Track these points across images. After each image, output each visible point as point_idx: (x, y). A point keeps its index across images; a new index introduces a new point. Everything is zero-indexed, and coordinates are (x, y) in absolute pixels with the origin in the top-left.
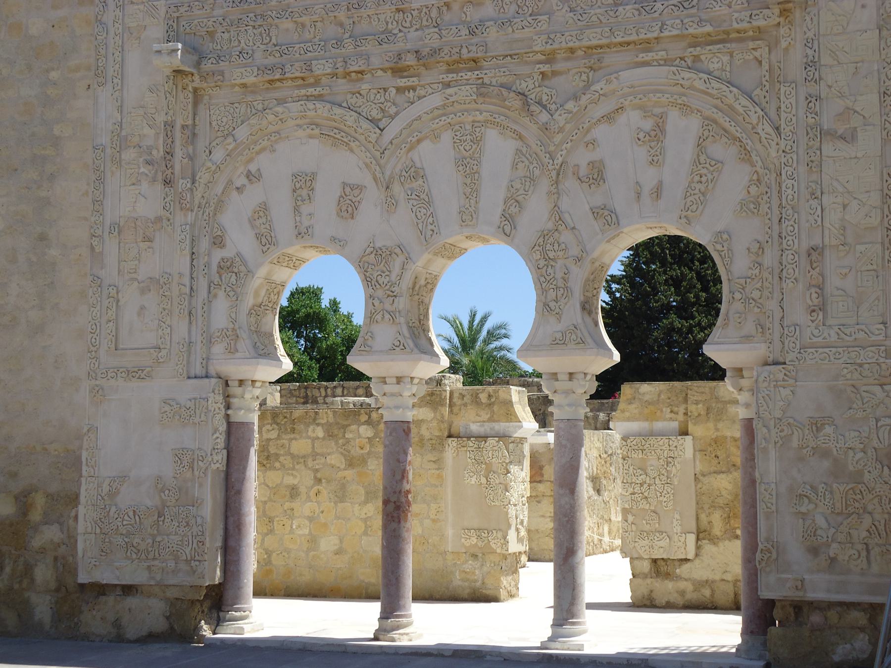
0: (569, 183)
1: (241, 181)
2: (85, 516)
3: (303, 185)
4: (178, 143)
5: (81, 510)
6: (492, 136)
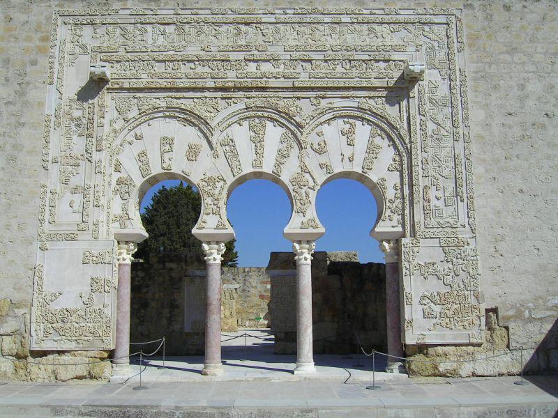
1: (130, 137)
3: (167, 142)
6: (269, 124)
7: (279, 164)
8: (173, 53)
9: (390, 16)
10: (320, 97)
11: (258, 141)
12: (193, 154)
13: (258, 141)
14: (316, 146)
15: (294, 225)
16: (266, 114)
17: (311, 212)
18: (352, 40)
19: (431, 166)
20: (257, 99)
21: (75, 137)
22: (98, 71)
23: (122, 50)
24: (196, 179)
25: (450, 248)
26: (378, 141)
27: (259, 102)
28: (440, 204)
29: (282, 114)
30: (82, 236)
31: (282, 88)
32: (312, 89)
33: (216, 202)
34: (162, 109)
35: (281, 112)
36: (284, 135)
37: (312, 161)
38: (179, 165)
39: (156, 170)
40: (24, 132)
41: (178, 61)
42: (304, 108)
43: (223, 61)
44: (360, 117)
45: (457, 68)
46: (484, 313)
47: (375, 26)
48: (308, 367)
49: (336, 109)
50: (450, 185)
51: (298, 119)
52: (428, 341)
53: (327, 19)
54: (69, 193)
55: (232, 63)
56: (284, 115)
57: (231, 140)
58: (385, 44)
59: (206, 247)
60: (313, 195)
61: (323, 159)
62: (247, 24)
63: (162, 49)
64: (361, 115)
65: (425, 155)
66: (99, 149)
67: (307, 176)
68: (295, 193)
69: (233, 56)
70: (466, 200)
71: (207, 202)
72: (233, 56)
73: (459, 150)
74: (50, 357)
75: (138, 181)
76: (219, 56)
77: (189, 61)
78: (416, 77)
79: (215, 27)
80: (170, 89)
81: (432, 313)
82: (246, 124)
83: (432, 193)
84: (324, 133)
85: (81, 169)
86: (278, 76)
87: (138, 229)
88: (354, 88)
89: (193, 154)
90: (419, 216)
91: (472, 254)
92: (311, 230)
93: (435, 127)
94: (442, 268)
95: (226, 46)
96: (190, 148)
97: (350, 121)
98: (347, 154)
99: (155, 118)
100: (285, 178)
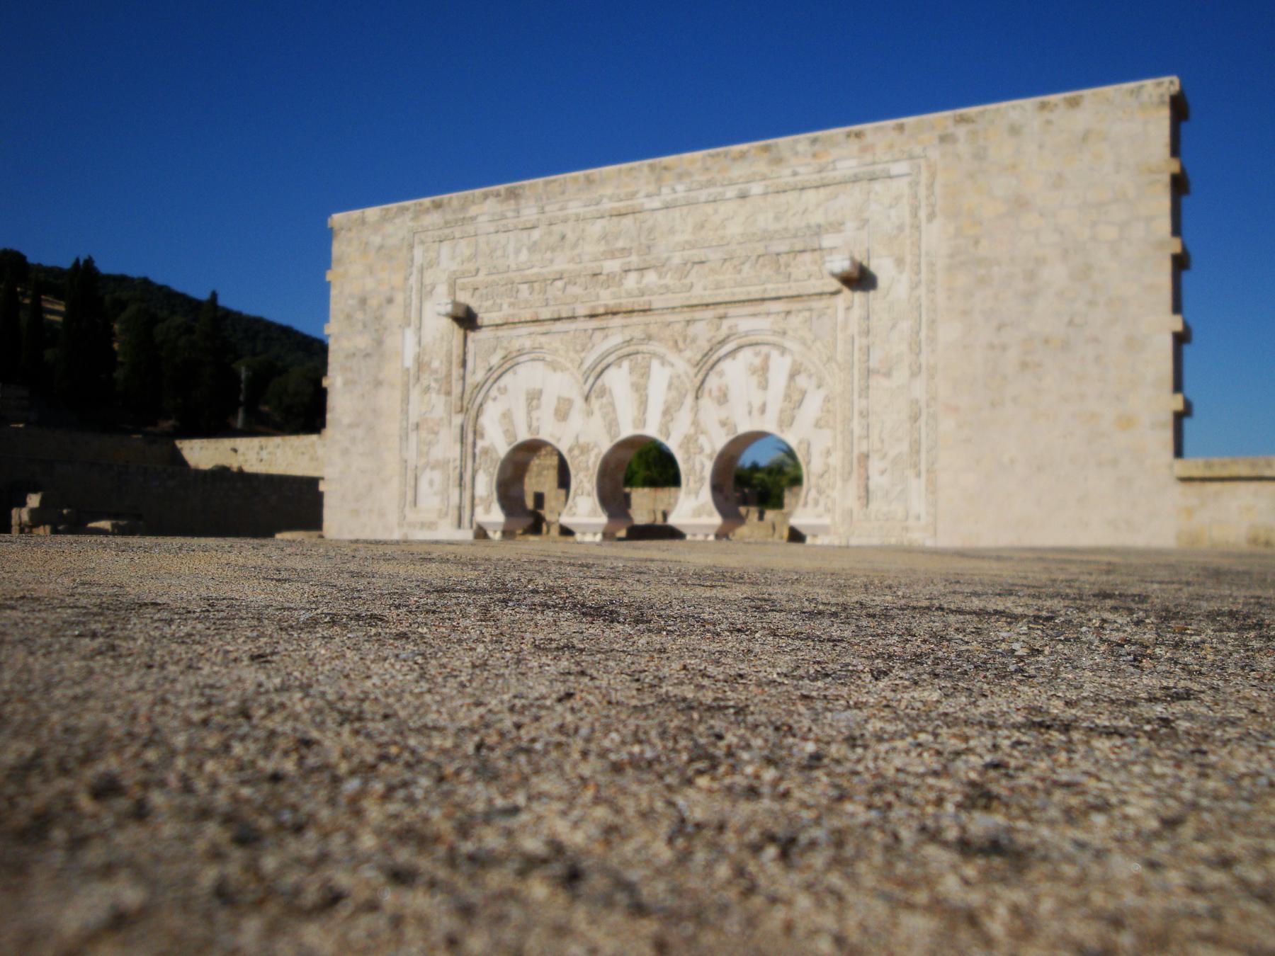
0: (706, 402)
3: (534, 397)
6: (655, 364)
11: (640, 389)
13: (640, 389)
61: (723, 413)
75: (503, 450)
82: (626, 364)
88: (763, 300)
89: (562, 414)
97: (764, 349)
98: (757, 404)
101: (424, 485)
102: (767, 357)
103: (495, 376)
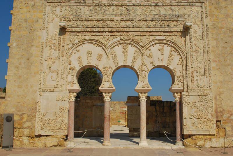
2: (37, 120)
4: (61, 42)
5: (37, 119)
6: (130, 46)
7: (133, 62)
8: (92, 17)
9: (178, 3)
10: (150, 35)
11: (125, 53)
12: (99, 57)
13: (125, 53)
14: (148, 55)
15: (140, 86)
16: (128, 42)
17: (146, 81)
18: (162, 12)
19: (194, 63)
20: (125, 36)
21: (53, 51)
22: (62, 25)
23: (72, 16)
24: (100, 68)
25: (202, 96)
26: (173, 53)
27: (126, 37)
28: (198, 78)
29: (135, 42)
30: (56, 90)
31: (135, 32)
32: (147, 32)
33: (108, 77)
34: (87, 40)
35: (134, 41)
36: (136, 51)
37: (147, 60)
38: (94, 63)
39: (85, 64)
40: (33, 49)
41: (94, 21)
42: (144, 40)
43: (111, 21)
44: (166, 43)
45: (205, 24)
46: (215, 122)
47: (172, 7)
48: (144, 142)
49: (156, 40)
50: (202, 70)
51: (141, 44)
52: (193, 133)
53: (153, 4)
54: (51, 73)
55: (115, 22)
56: (136, 42)
57: (115, 52)
58: (176, 14)
59: (104, 94)
60: (147, 74)
61: (151, 60)
62: (121, 6)
63: (87, 16)
64: (166, 43)
65: (192, 59)
66: (63, 55)
67: (145, 67)
68: (140, 74)
69: (115, 19)
70: (208, 75)
71: (105, 77)
72: (115, 19)
73: (206, 57)
74: (43, 138)
75: (78, 68)
76: (110, 19)
77: (98, 21)
78: (188, 28)
79: (108, 7)
80: (91, 32)
81: (195, 122)
82: (121, 46)
83: (195, 74)
84: (151, 50)
85: (55, 64)
86: (133, 27)
87: (77, 87)
89: (99, 57)
90: (190, 83)
91: (211, 98)
92: (146, 88)
93: (196, 47)
94: (198, 104)
95: (112, 15)
96: (98, 55)
97: (162, 45)
99: (84, 43)
100: (136, 68)
101: (48, 77)
102: (163, 47)
103: (76, 46)
